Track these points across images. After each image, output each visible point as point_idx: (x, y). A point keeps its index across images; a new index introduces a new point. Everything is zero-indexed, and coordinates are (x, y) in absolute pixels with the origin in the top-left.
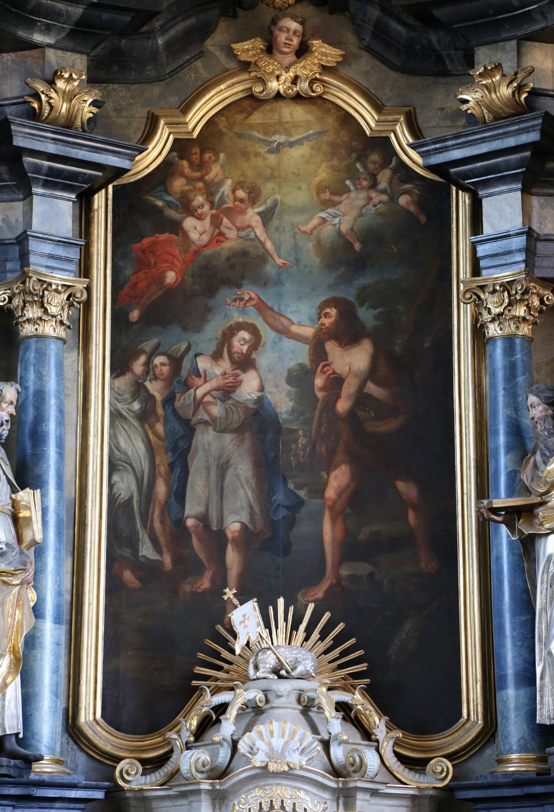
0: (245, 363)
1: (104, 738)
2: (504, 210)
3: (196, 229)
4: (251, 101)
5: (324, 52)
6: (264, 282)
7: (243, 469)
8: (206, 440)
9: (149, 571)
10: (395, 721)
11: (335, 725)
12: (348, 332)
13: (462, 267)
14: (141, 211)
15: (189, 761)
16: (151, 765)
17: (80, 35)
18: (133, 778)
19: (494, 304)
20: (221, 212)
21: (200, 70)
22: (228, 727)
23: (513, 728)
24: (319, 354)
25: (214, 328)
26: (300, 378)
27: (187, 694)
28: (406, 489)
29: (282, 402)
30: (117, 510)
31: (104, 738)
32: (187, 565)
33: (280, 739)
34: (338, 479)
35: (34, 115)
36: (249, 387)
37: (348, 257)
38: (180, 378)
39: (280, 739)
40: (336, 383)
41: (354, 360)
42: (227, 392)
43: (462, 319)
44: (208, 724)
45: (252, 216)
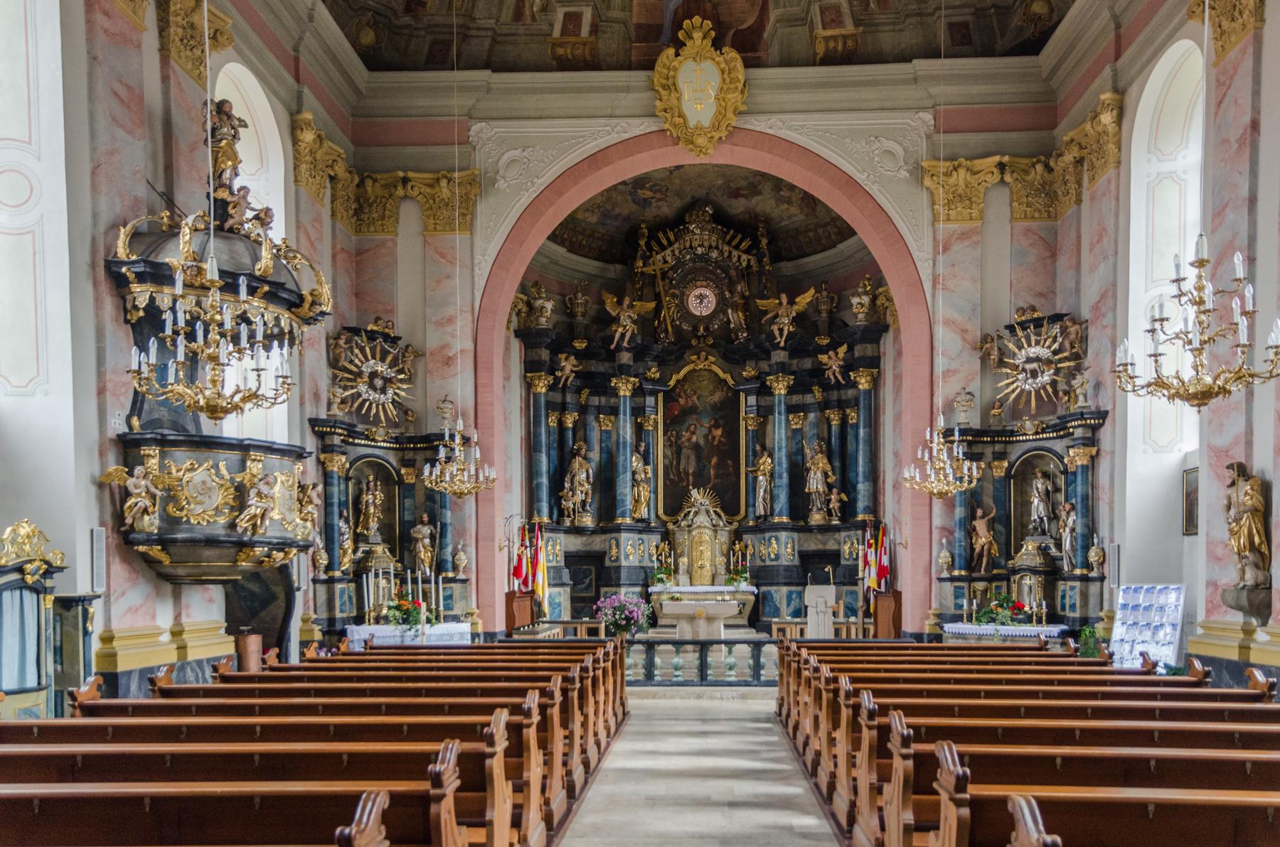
0: (693, 433)
1: (664, 518)
2: (752, 400)
3: (682, 401)
4: (694, 370)
5: (712, 359)
6: (698, 414)
7: (693, 457)
8: (685, 451)
9: (672, 481)
10: (726, 513)
11: (714, 516)
12: (716, 426)
13: (742, 414)
14: (670, 397)
15: (683, 523)
16: (675, 523)
17: (655, 358)
18: (671, 526)
19: (750, 422)
20: (688, 397)
21: (682, 362)
22: (691, 516)
23: (751, 516)
24: (710, 431)
25: (686, 425)
26: (706, 437)
27: (681, 508)
28: (730, 462)
29: (702, 442)
30: (665, 467)
31: (664, 518)
32: (681, 480)
33: (702, 519)
34: (714, 460)
35: (646, 379)
36: (694, 439)
37: (716, 408)
38: (678, 437)
39: (702, 519)
40: (714, 438)
41: (718, 432)
42: (689, 440)
43: (742, 424)
44: (687, 515)
45: (695, 398)
